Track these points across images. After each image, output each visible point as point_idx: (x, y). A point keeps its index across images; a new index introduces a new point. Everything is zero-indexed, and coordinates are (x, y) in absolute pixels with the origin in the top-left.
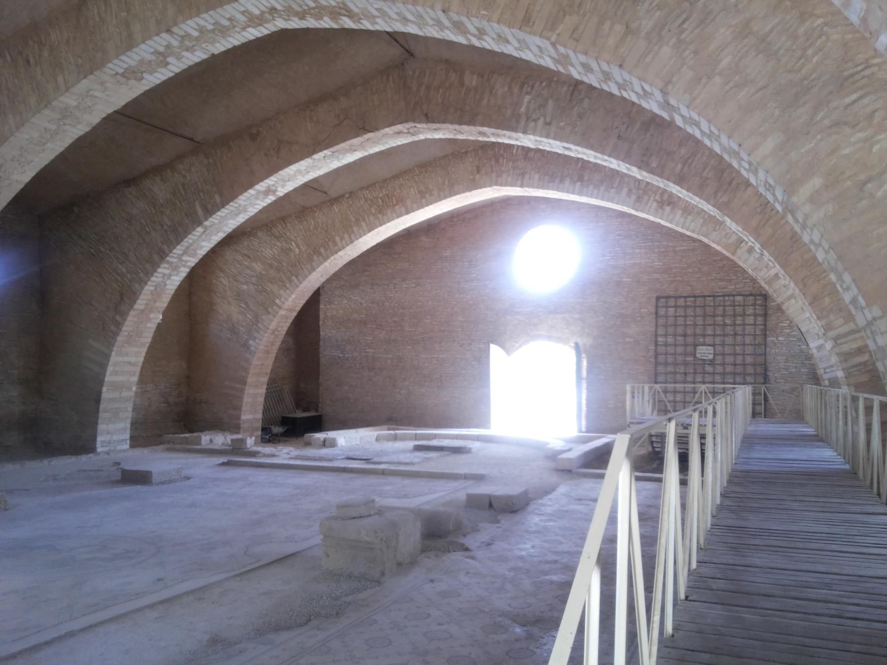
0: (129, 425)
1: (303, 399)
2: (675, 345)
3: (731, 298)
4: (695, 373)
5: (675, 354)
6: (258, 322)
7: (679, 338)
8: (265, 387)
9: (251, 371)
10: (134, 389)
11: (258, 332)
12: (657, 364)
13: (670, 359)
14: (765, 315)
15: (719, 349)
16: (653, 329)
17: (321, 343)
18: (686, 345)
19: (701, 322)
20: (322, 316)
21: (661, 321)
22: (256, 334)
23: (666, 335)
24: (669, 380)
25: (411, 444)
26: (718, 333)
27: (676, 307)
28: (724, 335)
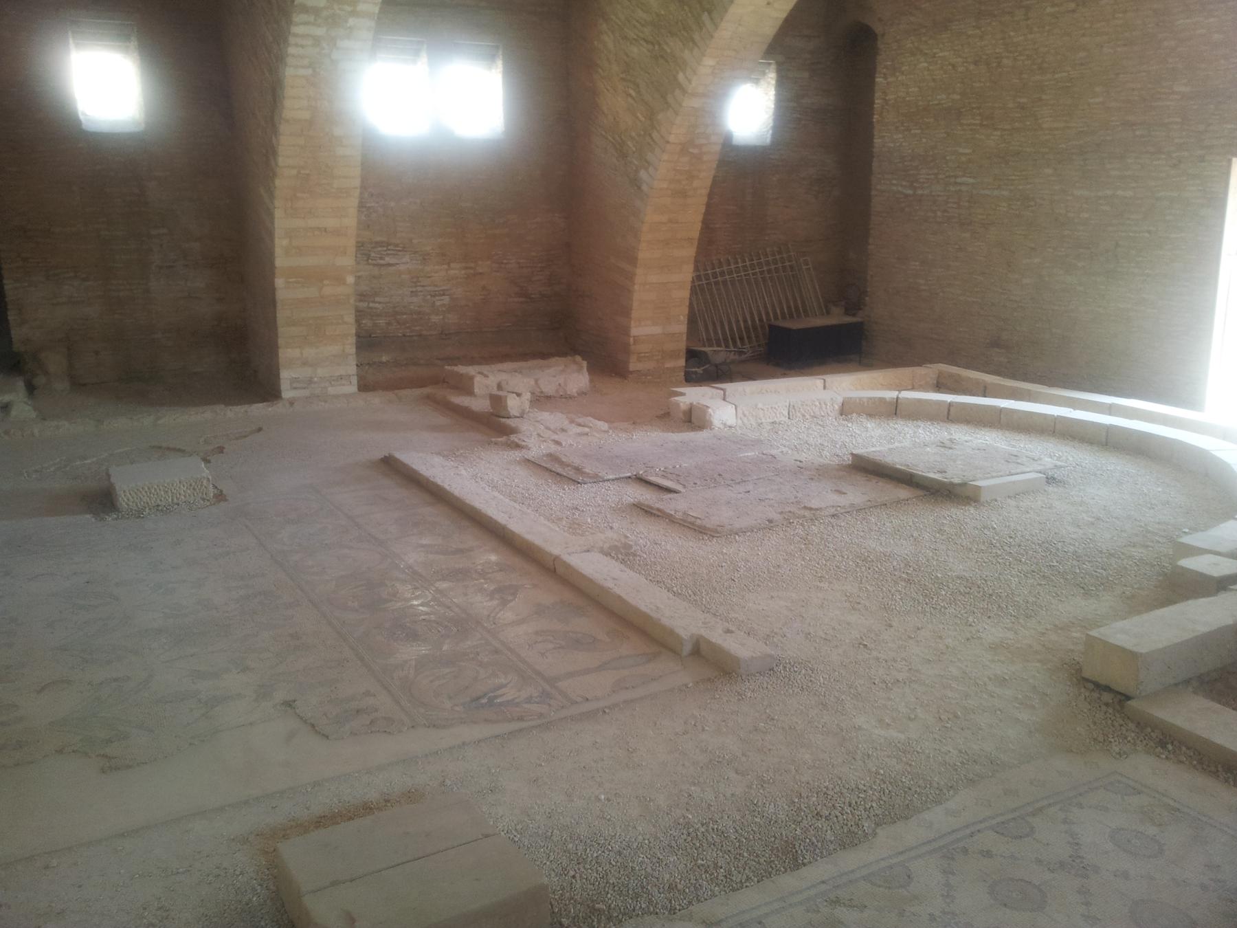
0: (351, 349)
1: (848, 285)
8: (691, 267)
10: (350, 279)
17: (875, 164)
20: (878, 102)
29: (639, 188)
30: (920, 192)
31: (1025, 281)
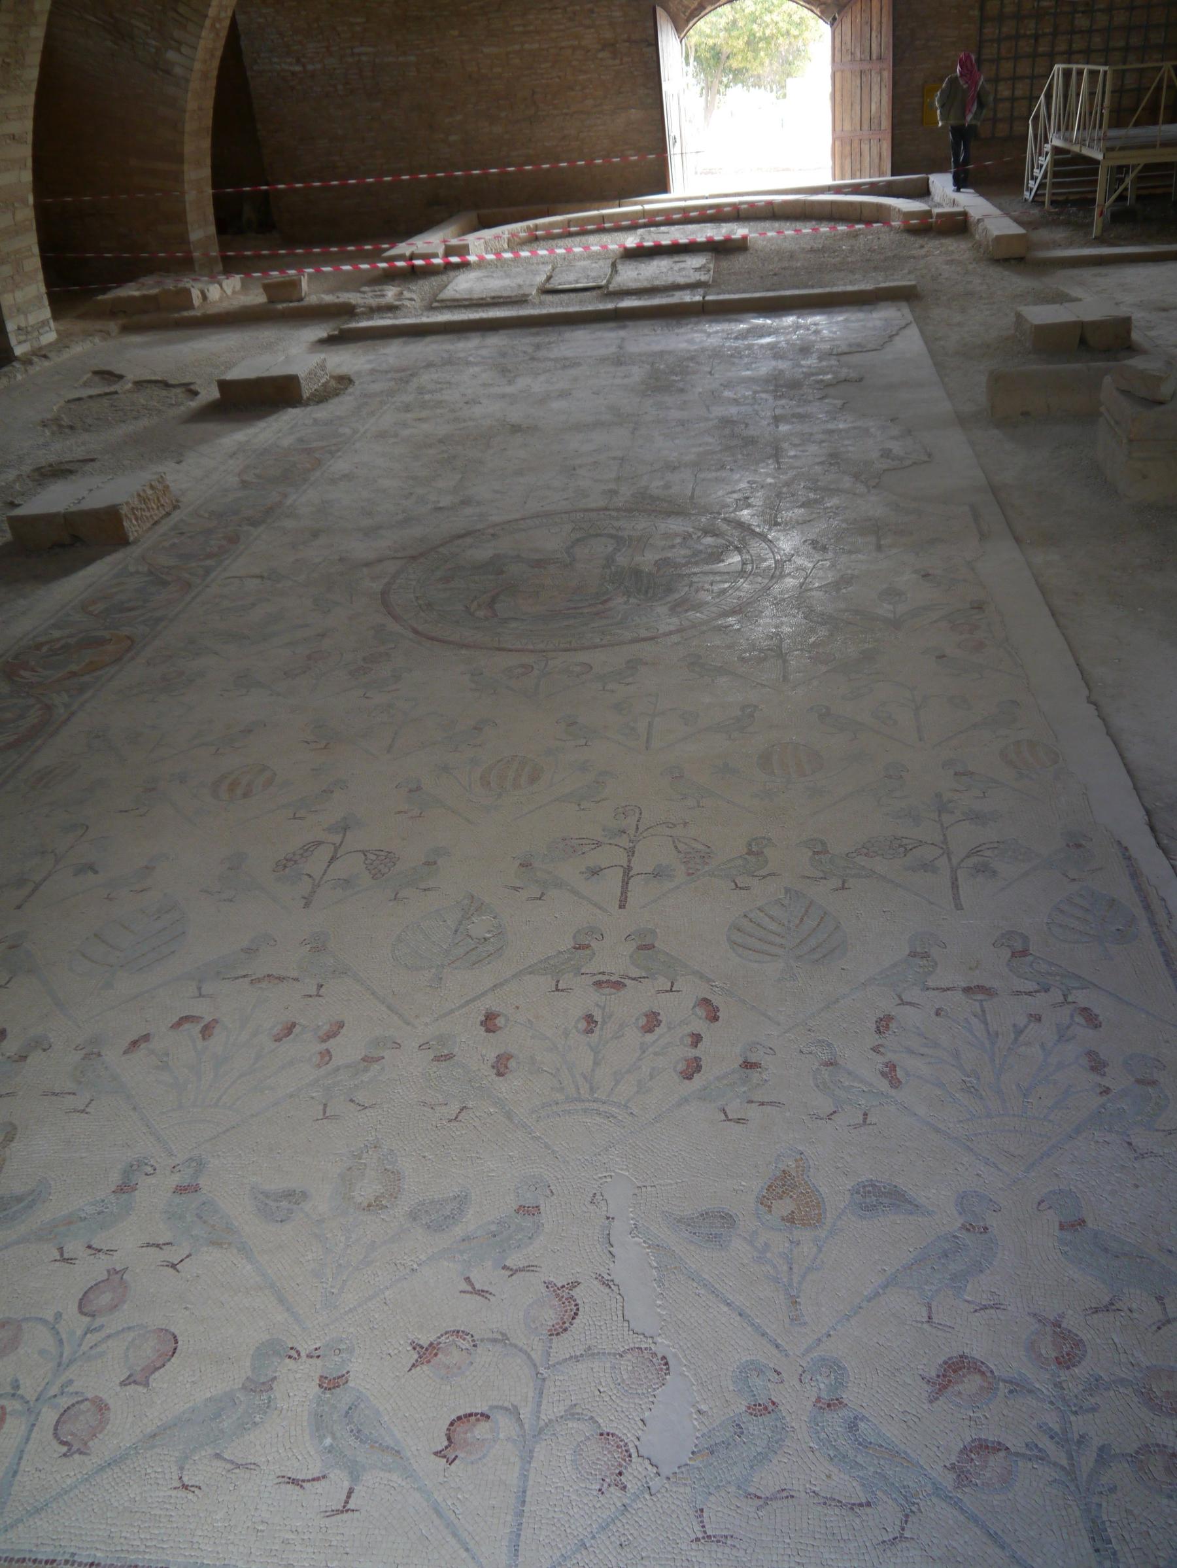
9: (189, 127)
10: (31, 199)
29: (168, 72)
30: (310, 67)
31: (452, 138)
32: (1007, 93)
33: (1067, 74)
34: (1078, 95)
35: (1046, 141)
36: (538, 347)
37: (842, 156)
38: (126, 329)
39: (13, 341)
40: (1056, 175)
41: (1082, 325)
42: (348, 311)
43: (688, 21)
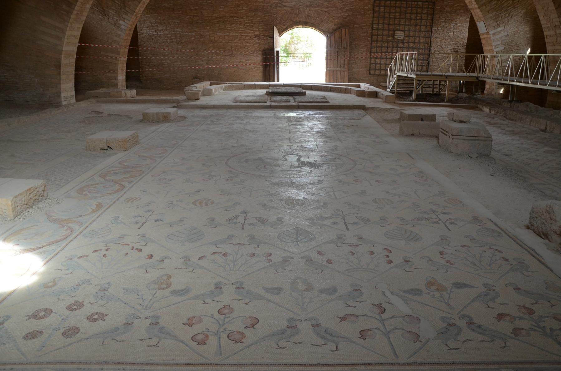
2: (383, 30)
3: (416, 3)
4: (393, 47)
5: (383, 35)
6: (126, 7)
7: (385, 26)
11: (126, 14)
12: (372, 41)
13: (380, 38)
14: (433, 14)
15: (407, 33)
16: (371, 19)
18: (389, 30)
19: (398, 17)
21: (376, 15)
22: (124, 16)
23: (378, 24)
24: (378, 50)
25: (264, 91)
26: (407, 24)
27: (385, 6)
28: (410, 25)
30: (159, 33)
32: (379, 62)
33: (402, 55)
34: (406, 59)
35: (395, 74)
36: (247, 113)
37: (330, 74)
38: (98, 102)
39: (63, 100)
40: (398, 84)
41: (422, 115)
42: (178, 101)
43: (283, 32)
